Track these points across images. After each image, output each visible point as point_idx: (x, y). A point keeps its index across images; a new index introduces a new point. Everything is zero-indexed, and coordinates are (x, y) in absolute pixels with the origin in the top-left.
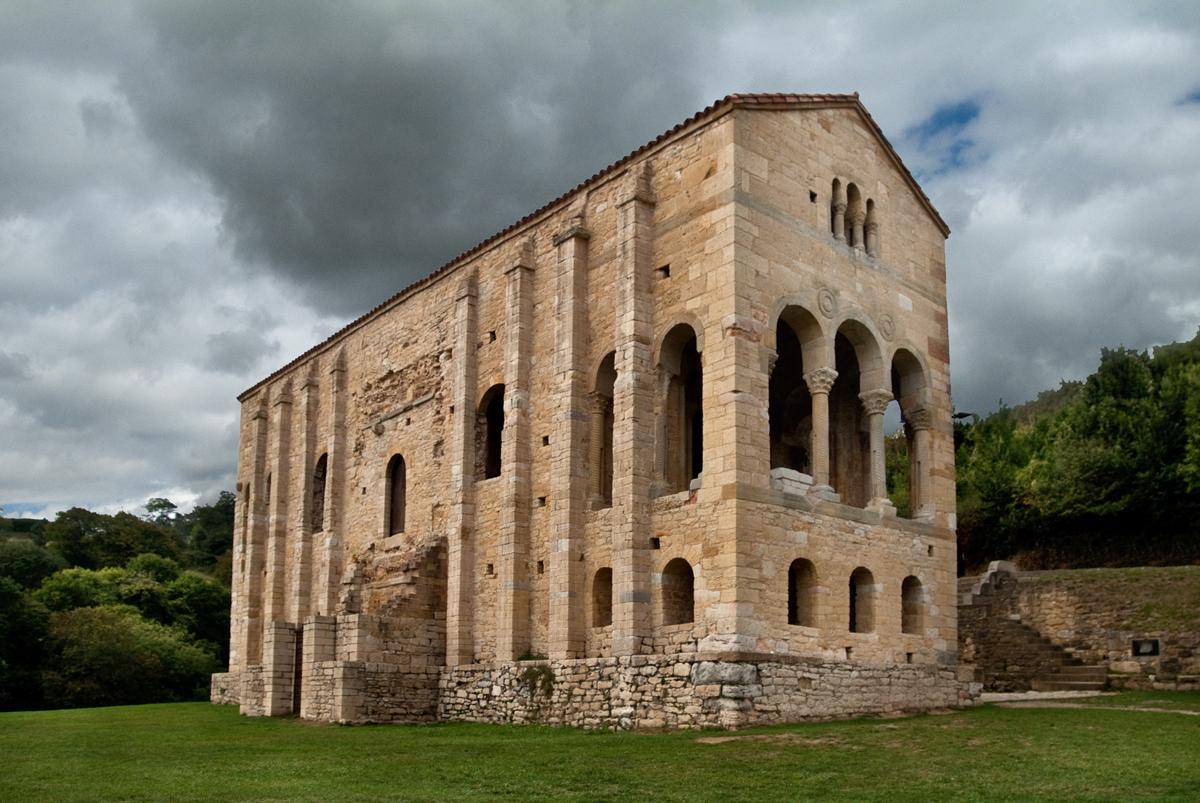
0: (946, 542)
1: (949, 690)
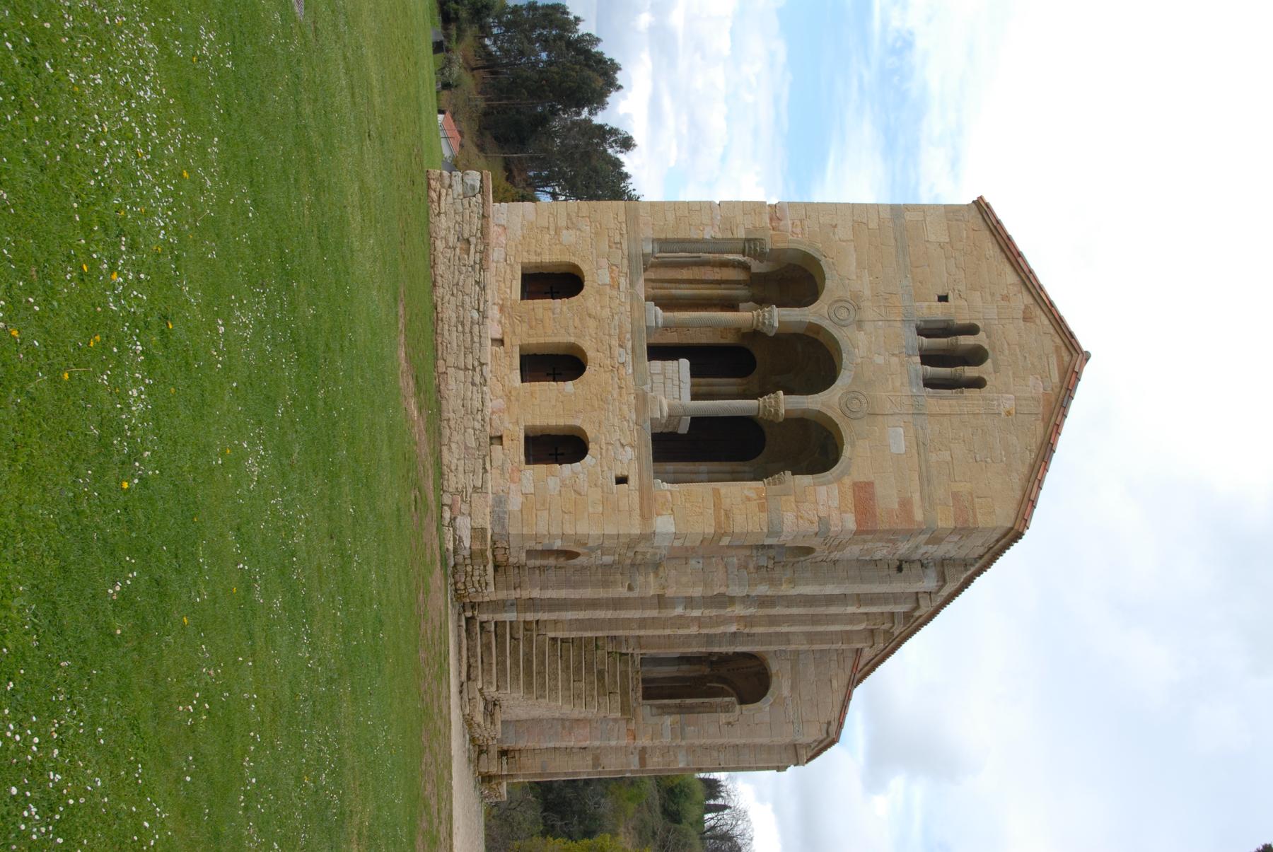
0: (637, 506)
1: (461, 476)
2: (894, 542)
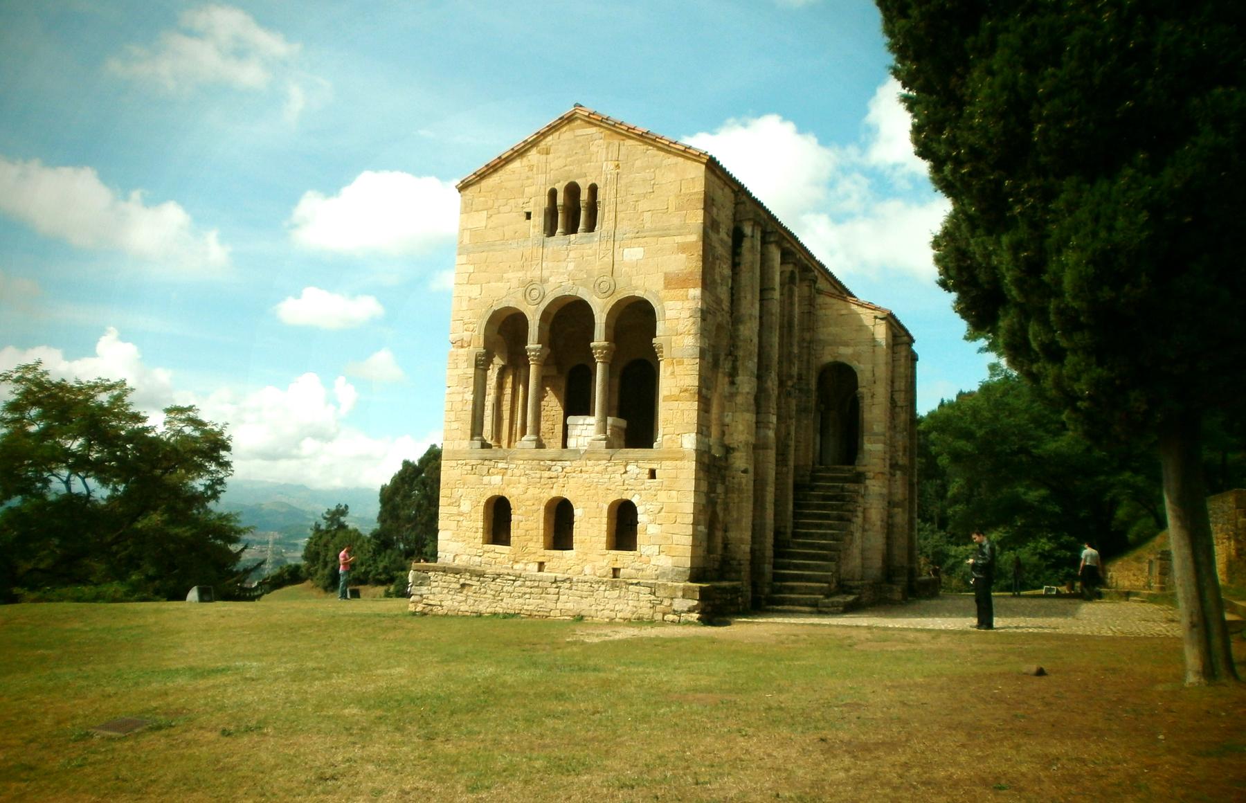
2: (716, 258)
